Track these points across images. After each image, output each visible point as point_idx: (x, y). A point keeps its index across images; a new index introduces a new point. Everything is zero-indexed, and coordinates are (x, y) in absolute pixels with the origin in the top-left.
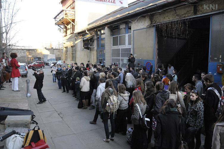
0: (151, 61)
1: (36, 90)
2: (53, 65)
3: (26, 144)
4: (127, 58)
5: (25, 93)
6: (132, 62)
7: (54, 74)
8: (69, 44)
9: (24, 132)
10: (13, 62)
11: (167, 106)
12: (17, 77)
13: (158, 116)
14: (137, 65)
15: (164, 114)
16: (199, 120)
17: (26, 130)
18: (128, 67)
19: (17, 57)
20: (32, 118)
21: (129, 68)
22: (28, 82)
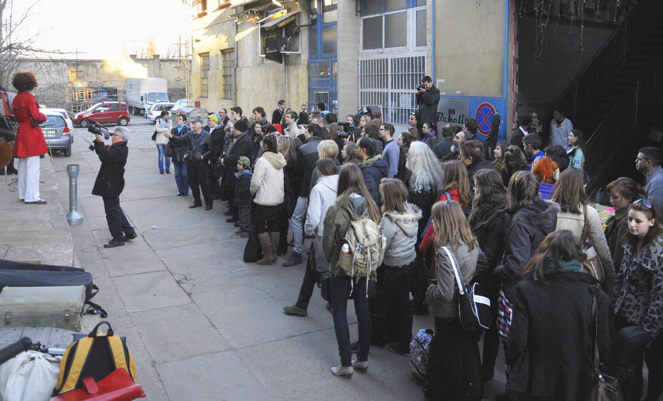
0: (492, 100)
1: (100, 200)
2: (159, 113)
3: (67, 383)
4: (411, 91)
5: (63, 209)
6: (428, 105)
7: (164, 146)
8: (215, 43)
9: (59, 342)
10: (23, 105)
11: (550, 255)
12: (36, 155)
13: (517, 288)
14: (446, 116)
15: (540, 283)
16: (658, 302)
17: (67, 337)
18: (415, 121)
19: (37, 88)
20: (89, 295)
21: (419, 126)
22: (72, 174)
